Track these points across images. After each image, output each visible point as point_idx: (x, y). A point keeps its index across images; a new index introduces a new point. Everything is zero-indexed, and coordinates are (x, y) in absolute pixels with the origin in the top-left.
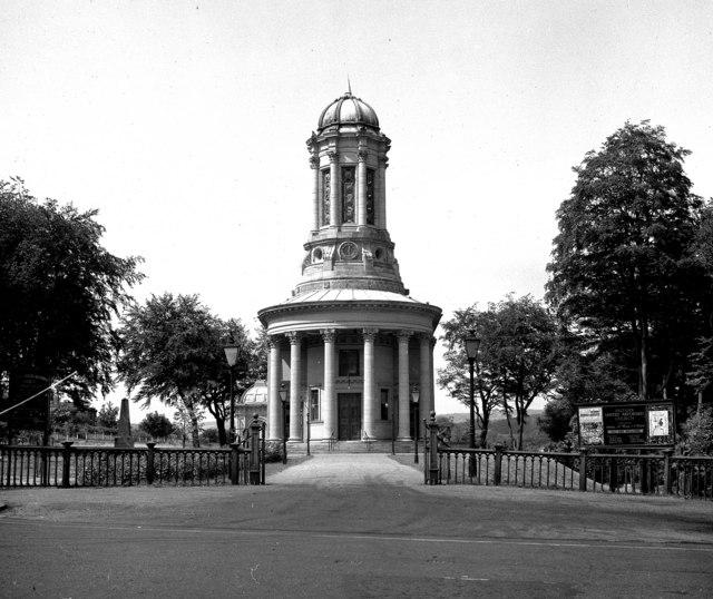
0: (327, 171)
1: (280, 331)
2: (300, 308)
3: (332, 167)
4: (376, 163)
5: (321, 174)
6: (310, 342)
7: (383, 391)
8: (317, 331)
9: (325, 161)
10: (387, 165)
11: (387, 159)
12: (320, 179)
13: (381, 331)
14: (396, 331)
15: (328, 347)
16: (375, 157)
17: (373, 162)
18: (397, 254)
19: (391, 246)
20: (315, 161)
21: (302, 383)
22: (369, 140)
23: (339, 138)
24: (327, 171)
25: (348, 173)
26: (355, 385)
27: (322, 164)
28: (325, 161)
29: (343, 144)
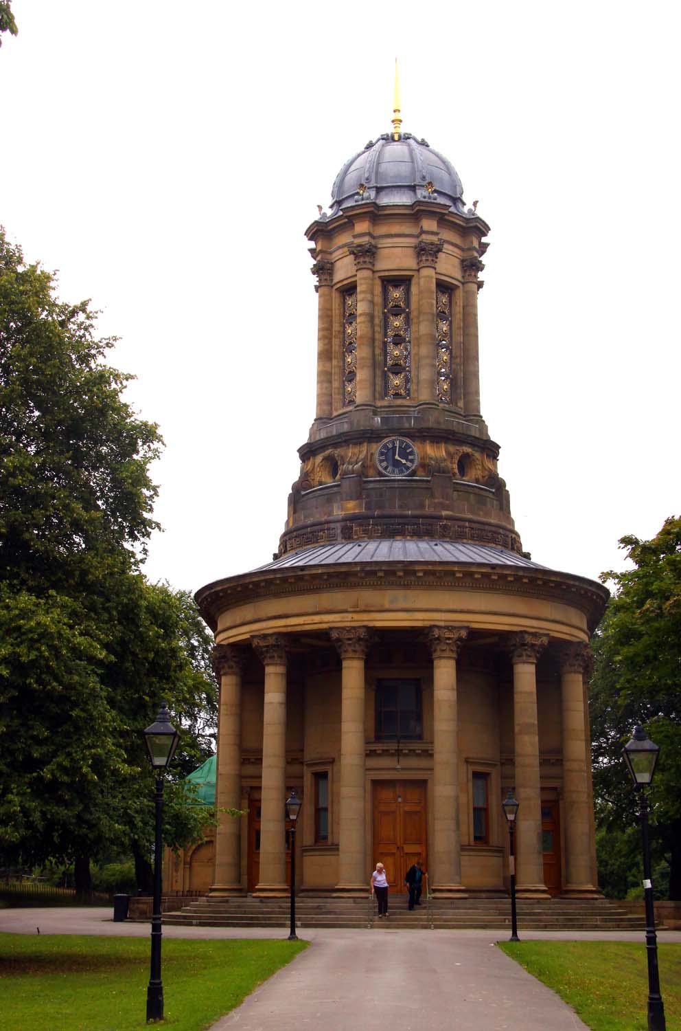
0: (349, 290)
1: (241, 634)
2: (284, 580)
3: (363, 279)
4: (457, 274)
5: (336, 297)
6: (312, 660)
7: (477, 775)
8: (323, 635)
9: (344, 268)
10: (480, 285)
11: (478, 267)
12: (336, 310)
13: (474, 634)
14: (504, 636)
16: (456, 262)
17: (448, 265)
18: (505, 468)
19: (492, 450)
20: (323, 270)
21: (293, 756)
22: (443, 219)
23: (376, 214)
24: (349, 290)
25: (396, 294)
26: (413, 762)
27: (335, 281)
28: (344, 268)
29: (382, 230)
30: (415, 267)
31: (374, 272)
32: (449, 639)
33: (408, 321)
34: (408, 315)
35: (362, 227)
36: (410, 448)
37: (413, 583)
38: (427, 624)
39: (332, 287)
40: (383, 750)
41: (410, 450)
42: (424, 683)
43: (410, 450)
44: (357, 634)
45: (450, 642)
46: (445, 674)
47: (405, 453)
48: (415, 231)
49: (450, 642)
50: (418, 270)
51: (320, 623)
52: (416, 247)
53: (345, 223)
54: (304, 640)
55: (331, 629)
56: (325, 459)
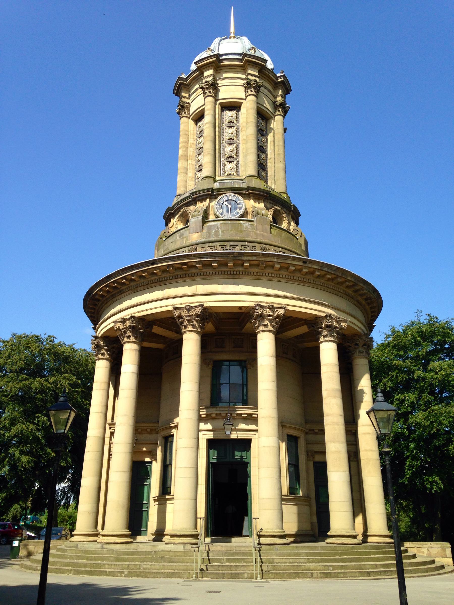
15: (191, 344)
30: (245, 98)
31: (216, 100)
32: (269, 316)
33: (238, 130)
34: (238, 127)
35: (208, 73)
36: (239, 200)
37: (241, 273)
38: (253, 305)
39: (189, 118)
40: (217, 414)
41: (240, 201)
42: (249, 363)
43: (240, 201)
44: (195, 313)
45: (271, 318)
46: (266, 344)
47: (236, 205)
48: (244, 76)
49: (271, 318)
50: (245, 99)
51: (167, 306)
52: (244, 84)
53: (198, 75)
54: (156, 330)
55: (175, 308)
56: (181, 215)
